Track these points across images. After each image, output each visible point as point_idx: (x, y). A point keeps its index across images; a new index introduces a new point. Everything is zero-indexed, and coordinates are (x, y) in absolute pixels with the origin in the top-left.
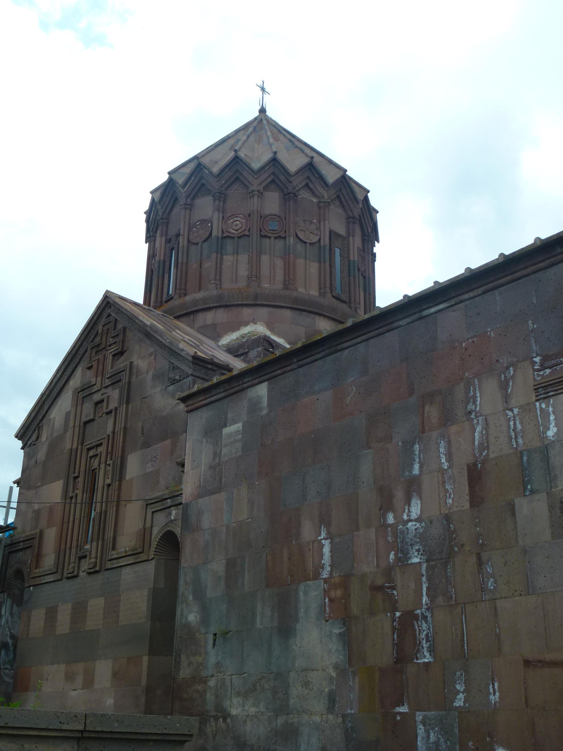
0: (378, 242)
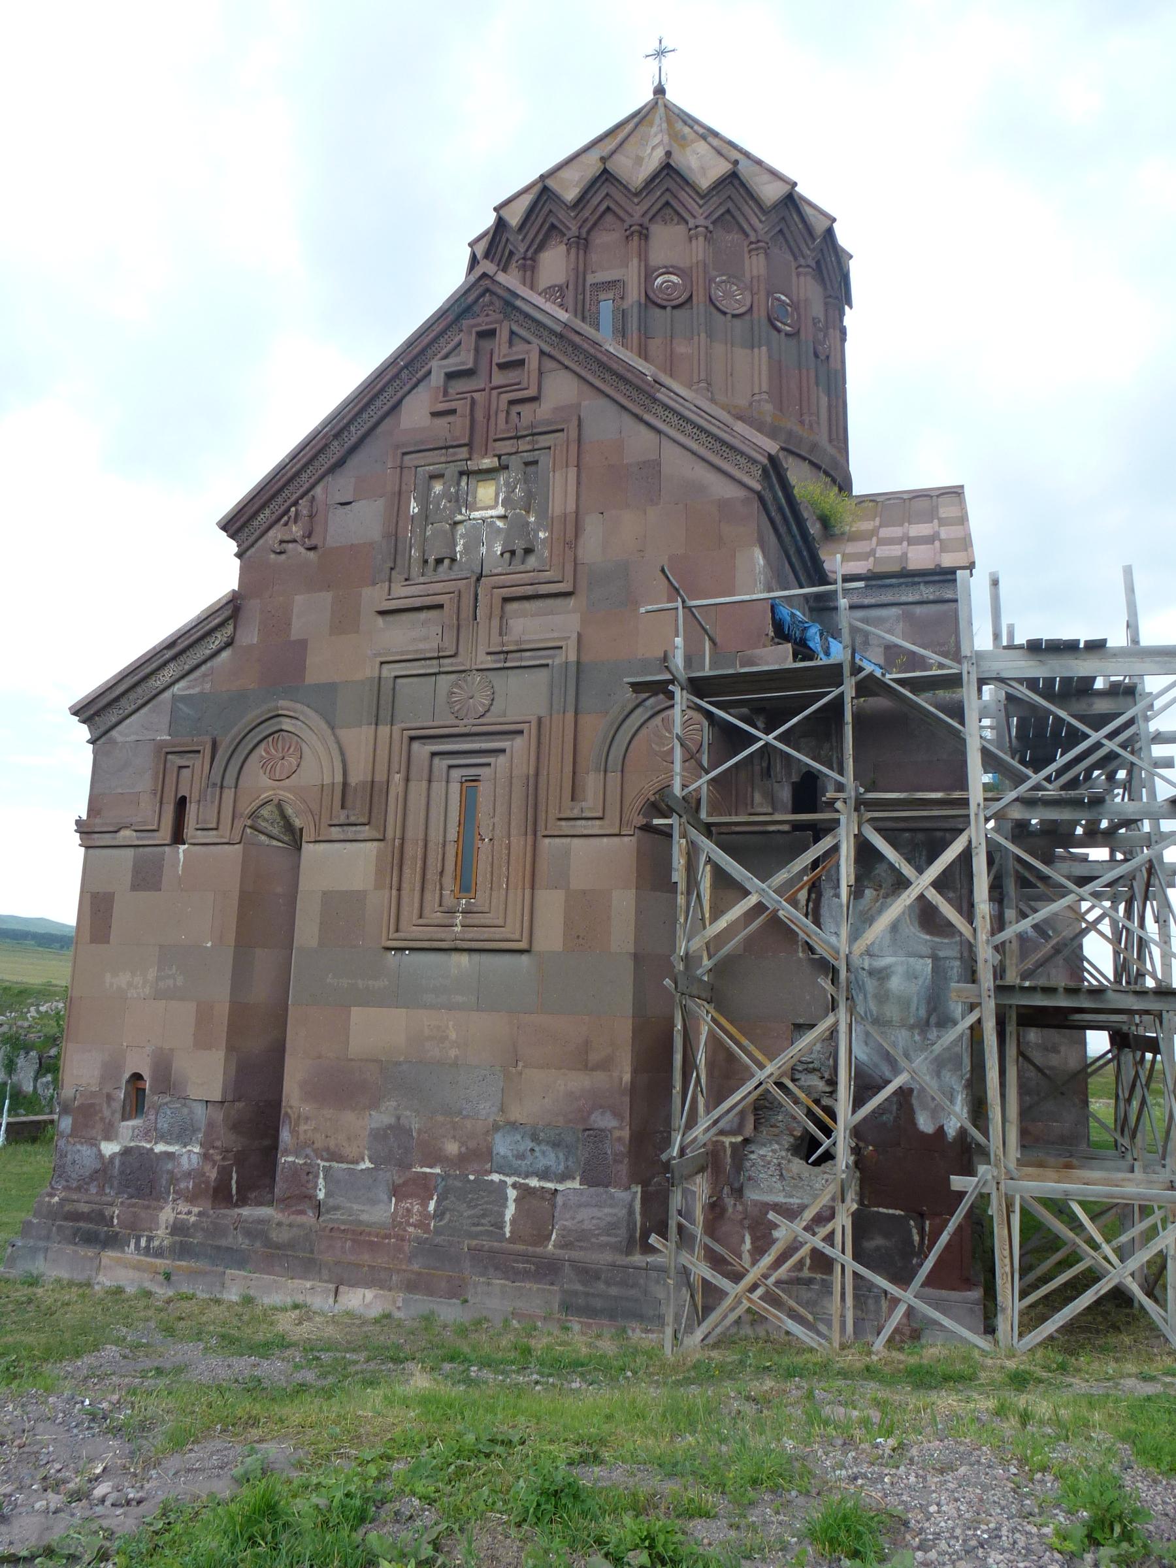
0: (851, 307)
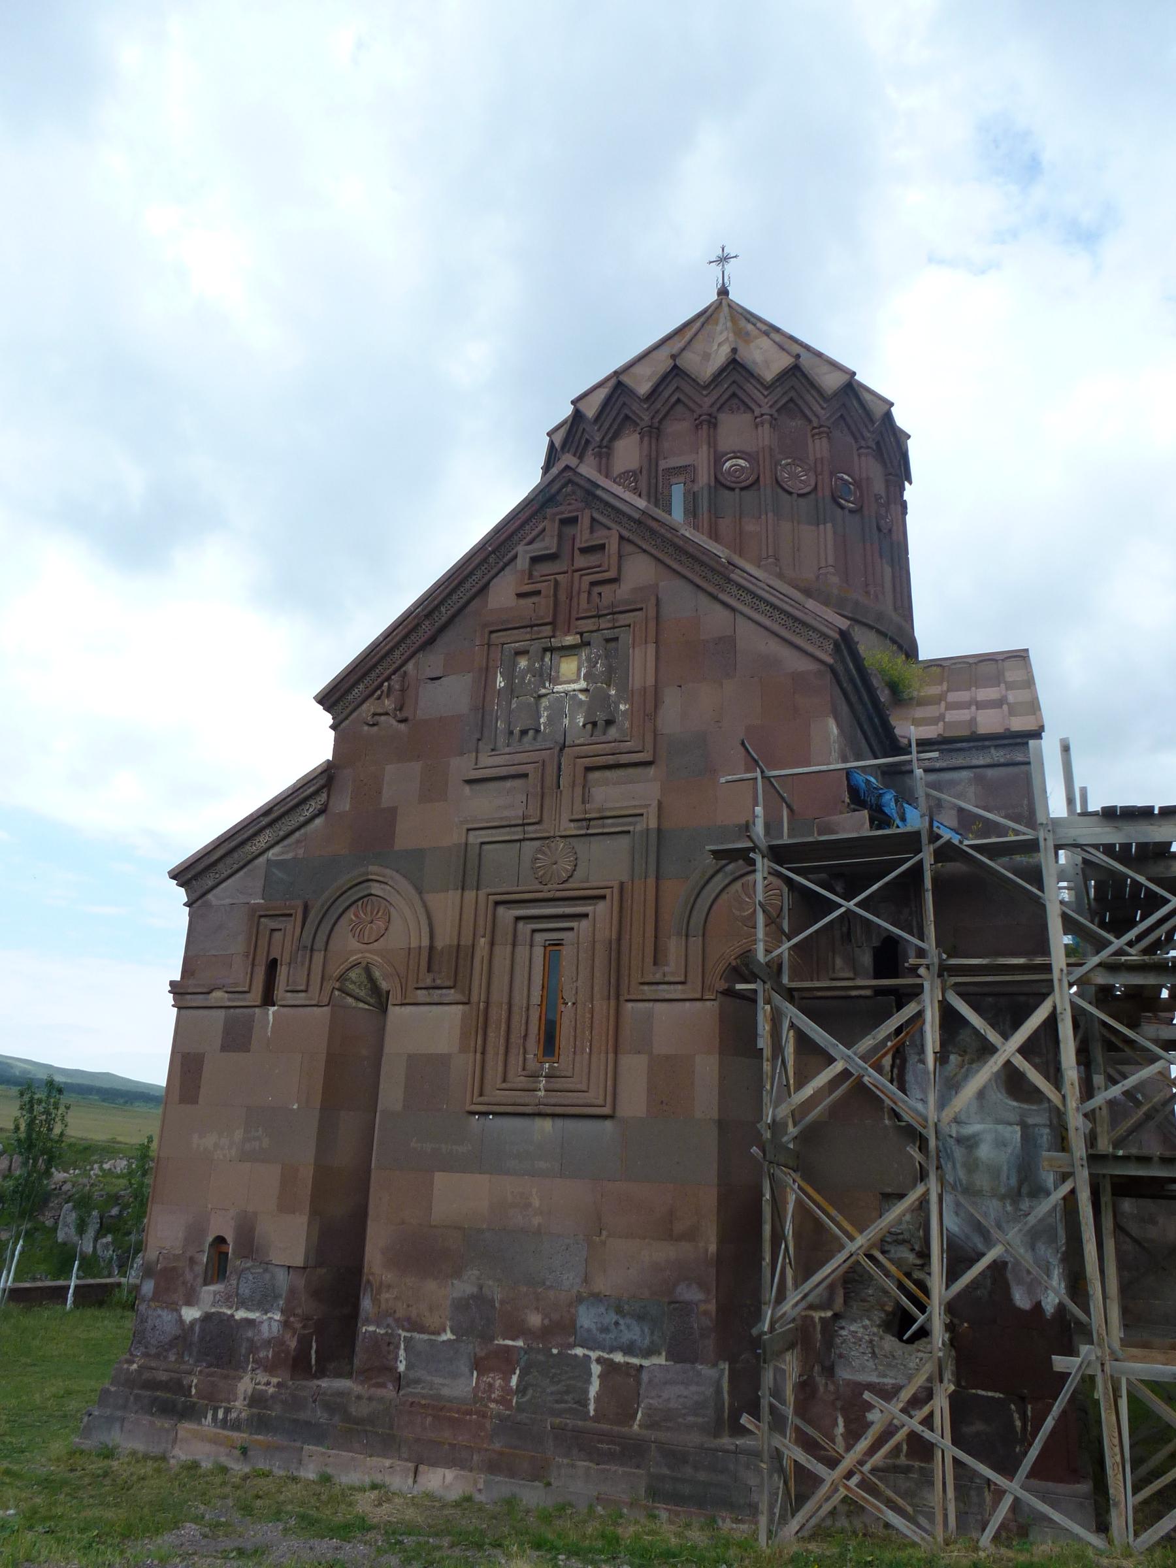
0: (910, 483)
